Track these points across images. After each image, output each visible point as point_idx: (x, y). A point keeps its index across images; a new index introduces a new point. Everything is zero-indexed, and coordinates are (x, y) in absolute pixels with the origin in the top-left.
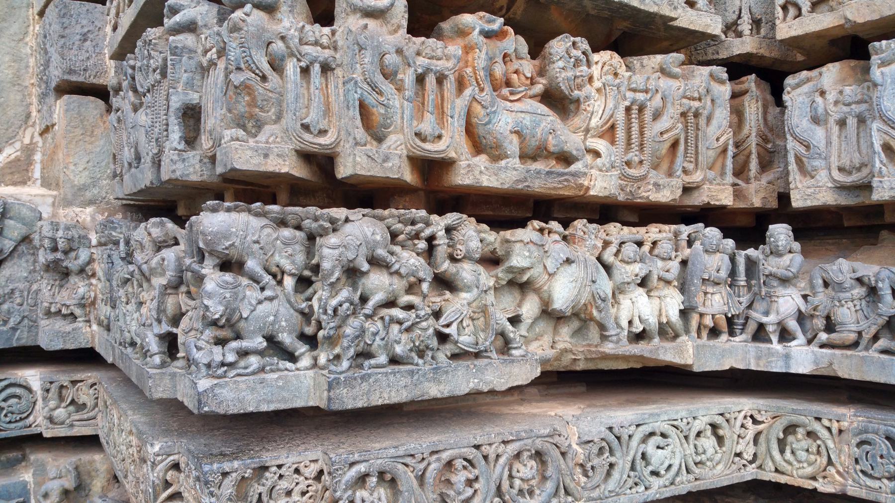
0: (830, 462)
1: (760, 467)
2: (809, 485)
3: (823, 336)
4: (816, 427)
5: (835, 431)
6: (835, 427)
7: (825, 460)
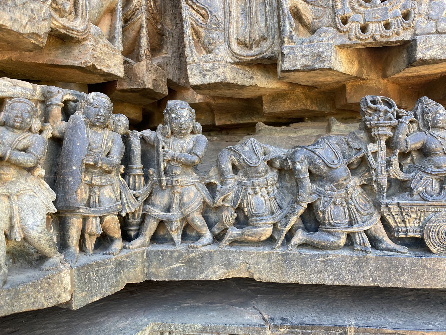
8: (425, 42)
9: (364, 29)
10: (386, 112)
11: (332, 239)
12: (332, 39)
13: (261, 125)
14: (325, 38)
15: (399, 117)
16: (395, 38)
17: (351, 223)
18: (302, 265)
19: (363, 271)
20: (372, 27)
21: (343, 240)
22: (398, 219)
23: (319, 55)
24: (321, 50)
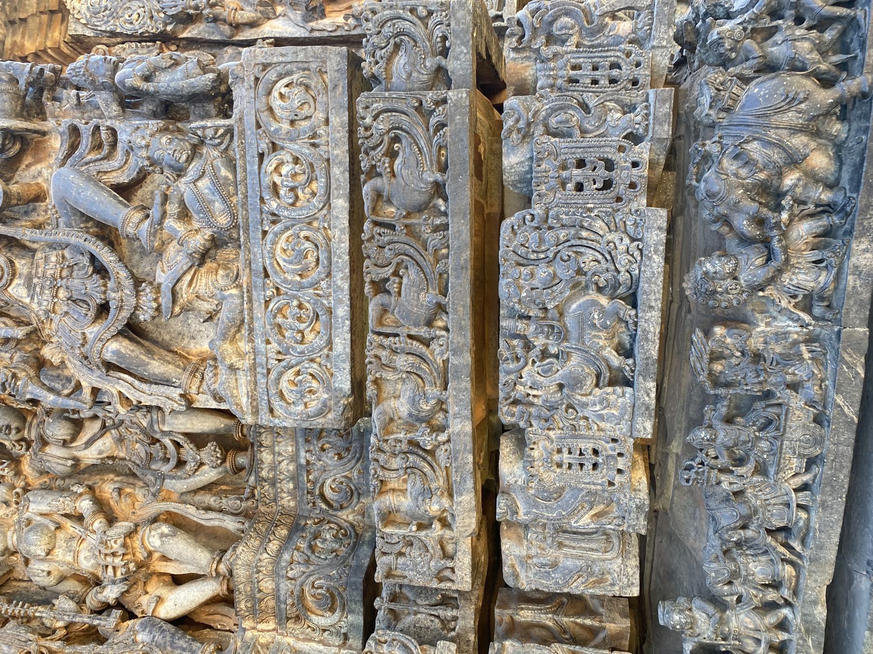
3: (786, 593)
8: (639, 432)
9: (620, 471)
10: (697, 473)
11: (801, 523)
12: (625, 496)
17: (788, 505)
18: (821, 548)
19: (832, 505)
20: (620, 467)
21: (803, 515)
23: (638, 507)
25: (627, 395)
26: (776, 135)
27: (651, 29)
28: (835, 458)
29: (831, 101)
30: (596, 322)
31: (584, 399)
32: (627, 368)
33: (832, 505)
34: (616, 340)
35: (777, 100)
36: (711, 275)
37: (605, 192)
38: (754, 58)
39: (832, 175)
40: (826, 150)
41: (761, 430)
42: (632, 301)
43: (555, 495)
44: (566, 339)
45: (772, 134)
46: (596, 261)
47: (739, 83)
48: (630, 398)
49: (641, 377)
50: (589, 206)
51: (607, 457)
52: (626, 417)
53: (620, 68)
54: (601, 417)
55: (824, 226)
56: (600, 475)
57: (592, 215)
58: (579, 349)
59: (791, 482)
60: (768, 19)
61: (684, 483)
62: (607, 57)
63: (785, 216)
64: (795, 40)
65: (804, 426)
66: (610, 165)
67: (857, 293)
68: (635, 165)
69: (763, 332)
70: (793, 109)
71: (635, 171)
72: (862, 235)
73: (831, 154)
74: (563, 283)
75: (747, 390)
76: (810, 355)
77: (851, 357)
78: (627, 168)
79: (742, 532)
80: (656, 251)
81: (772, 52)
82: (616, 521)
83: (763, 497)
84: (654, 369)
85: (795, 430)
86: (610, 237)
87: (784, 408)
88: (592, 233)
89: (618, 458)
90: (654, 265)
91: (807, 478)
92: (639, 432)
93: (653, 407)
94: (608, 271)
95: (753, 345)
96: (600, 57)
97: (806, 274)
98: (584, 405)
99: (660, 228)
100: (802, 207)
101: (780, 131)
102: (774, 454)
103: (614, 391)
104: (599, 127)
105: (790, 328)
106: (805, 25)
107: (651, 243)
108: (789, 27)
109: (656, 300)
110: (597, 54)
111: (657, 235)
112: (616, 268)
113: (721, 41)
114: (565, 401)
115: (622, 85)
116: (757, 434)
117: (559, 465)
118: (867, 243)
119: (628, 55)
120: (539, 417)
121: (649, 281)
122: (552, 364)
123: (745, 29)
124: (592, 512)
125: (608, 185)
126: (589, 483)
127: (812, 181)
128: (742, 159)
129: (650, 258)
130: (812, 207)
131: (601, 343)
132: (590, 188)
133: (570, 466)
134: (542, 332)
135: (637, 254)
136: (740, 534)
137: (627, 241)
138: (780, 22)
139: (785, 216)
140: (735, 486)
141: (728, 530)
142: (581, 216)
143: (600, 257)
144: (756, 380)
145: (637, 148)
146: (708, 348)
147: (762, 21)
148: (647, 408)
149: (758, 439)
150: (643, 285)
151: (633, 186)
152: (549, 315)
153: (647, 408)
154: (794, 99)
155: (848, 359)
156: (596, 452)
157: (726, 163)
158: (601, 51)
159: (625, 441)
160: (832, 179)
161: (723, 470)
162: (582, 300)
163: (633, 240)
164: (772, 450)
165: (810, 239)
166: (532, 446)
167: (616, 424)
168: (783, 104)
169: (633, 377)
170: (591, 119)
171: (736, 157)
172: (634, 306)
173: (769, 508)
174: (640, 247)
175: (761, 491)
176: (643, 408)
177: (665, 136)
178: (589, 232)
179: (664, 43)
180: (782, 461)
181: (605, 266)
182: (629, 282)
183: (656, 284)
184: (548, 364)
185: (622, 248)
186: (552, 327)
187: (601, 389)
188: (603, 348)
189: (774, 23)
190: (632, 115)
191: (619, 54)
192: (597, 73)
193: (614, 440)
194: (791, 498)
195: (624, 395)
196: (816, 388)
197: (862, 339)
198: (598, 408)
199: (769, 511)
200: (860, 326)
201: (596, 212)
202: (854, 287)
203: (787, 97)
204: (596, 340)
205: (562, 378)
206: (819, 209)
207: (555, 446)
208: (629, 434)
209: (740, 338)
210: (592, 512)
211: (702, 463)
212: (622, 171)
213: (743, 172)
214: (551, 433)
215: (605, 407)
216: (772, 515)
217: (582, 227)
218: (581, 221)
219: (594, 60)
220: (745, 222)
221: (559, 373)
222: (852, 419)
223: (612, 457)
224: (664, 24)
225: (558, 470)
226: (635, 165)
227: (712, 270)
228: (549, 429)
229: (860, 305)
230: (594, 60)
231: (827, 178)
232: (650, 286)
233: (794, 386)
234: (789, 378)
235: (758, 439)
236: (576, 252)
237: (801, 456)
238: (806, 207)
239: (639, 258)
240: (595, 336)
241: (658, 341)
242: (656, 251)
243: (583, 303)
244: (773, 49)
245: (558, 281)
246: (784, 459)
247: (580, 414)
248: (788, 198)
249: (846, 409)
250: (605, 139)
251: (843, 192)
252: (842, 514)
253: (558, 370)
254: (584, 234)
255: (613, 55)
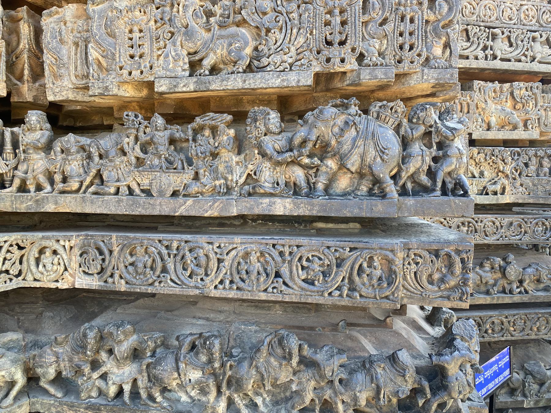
0: (66, 269)
1: (24, 279)
2: (53, 285)
3: (61, 186)
4: (56, 246)
5: (67, 247)
6: (67, 244)
7: (62, 268)
8: (159, 82)
9: (130, 73)
10: (133, 121)
11: (106, 189)
12: (114, 78)
13: (116, 126)
14: (111, 78)
15: (140, 124)
16: (145, 80)
17: (118, 180)
18: (92, 203)
19: (121, 206)
20: (133, 73)
21: (112, 190)
22: (140, 179)
23: (107, 87)
24: (107, 85)
25: (183, 73)
26: (361, 145)
27: (435, 68)
28: (151, 204)
29: (381, 176)
30: (233, 46)
31: (178, 43)
32: (202, 71)
33: (121, 206)
34: (222, 66)
35: (383, 143)
36: (268, 117)
37: (324, 41)
38: (412, 133)
39: (334, 191)
40: (350, 186)
41: (166, 159)
42: (249, 69)
43: (109, 30)
44: (221, 26)
45: (360, 142)
46: (276, 41)
47: (396, 123)
48: (182, 75)
49: (196, 79)
50: (314, 31)
51: (140, 63)
52: (168, 73)
53: (410, 50)
54: (167, 56)
55: (301, 185)
56: (126, 60)
57: (308, 35)
58: (213, 36)
59: (134, 182)
60: (437, 141)
61: (125, 113)
62: (418, 40)
63: (306, 161)
64: (422, 156)
65: (169, 185)
66: (342, 43)
67: (258, 205)
68: (343, 61)
69: (232, 160)
70: (377, 154)
71: (338, 60)
72: (295, 204)
73: (348, 190)
74: (260, 20)
75: (192, 147)
76: (217, 184)
77: (217, 207)
78: (340, 54)
79: (97, 154)
80: (283, 80)
81: (415, 145)
82: (95, 75)
83: (122, 167)
84: (203, 88)
85: (167, 179)
86: (293, 49)
87: (182, 171)
88: (295, 36)
89: (139, 71)
90: (274, 80)
91: (137, 191)
92: (159, 82)
93: (177, 90)
94: (269, 50)
95: (223, 155)
96: (418, 35)
97: (269, 175)
98: (174, 45)
99: (299, 81)
100: (313, 175)
101: (362, 147)
102: (151, 168)
103: (186, 63)
104: (369, 34)
105: (235, 175)
106: (432, 163)
107: (289, 77)
108: (431, 153)
109: (249, 84)
110: (420, 32)
111: (294, 80)
112: (271, 55)
113: (425, 109)
114: (176, 29)
115: (398, 52)
116: (163, 156)
117: (131, 31)
118: (290, 207)
119: (419, 55)
120: (163, 12)
121: (262, 78)
122: (202, 17)
123: (431, 126)
124: (100, 58)
125: (329, 43)
126: (120, 52)
127: (330, 177)
128: (344, 127)
129: (278, 77)
130: (314, 181)
131: (218, 51)
132: (327, 31)
133: (131, 39)
134: (224, 10)
135: (281, 68)
136: (95, 153)
137: (290, 61)
138: (435, 148)
139: (306, 161)
140: (127, 146)
141: (97, 145)
142: (307, 27)
143: (278, 44)
144: (199, 152)
145: (354, 60)
146: (219, 123)
147: (436, 137)
148: (175, 86)
149: (160, 157)
150: (259, 75)
151: (328, 60)
152: (237, 15)
153: (175, 86)
154: (383, 153)
155: (216, 205)
156: (141, 57)
157: (343, 118)
158: (422, 35)
159: (152, 75)
160: (331, 192)
161: (137, 139)
162: (249, 36)
163: (291, 65)
164: (153, 166)
165: (293, 179)
166: (142, 10)
167: (163, 67)
168: (381, 147)
169: (196, 76)
170: (375, 27)
171: (346, 123)
172: (244, 72)
173: (115, 170)
174: (286, 70)
175: (126, 166)
176: (175, 84)
177: (361, 78)
178: (296, 34)
179: (425, 77)
180: (146, 173)
181: (272, 47)
182: (262, 65)
183: (261, 83)
184: (202, 15)
185: (285, 58)
186: (228, 17)
187: (187, 55)
188: (215, 53)
189: (434, 144)
190: (377, 55)
191: (420, 47)
192: (407, 34)
193: (151, 68)
194: (123, 182)
195: (184, 70)
196: (196, 189)
197: (229, 212)
198: (173, 54)
199: (113, 170)
200: (237, 209)
201: (309, 36)
202: (262, 203)
203: (385, 149)
204: (220, 48)
205: (192, 27)
206: (312, 185)
207: (143, 27)
208: (157, 76)
209: (227, 144)
210: (100, 58)
211: (140, 124)
212: (339, 51)
213: (336, 130)
214: (152, 23)
215: (174, 58)
216: (110, 171)
217: (300, 29)
218: (303, 27)
219: (416, 31)
220: (303, 134)
221: (196, 25)
222: (178, 211)
223: (140, 66)
224: (438, 76)
225: (127, 31)
226: (343, 61)
227: (271, 117)
228: (156, 22)
229: (250, 208)
230: (416, 31)
231: (332, 189)
232: (259, 78)
233: (196, 177)
234: (201, 171)
235: (160, 157)
236: (281, 29)
237: (151, 184)
238: (313, 177)
239: (278, 70)
240: (223, 46)
241: (222, 88)
242: (283, 80)
243: (246, 36)
244: (417, 145)
245: (261, 16)
246: (148, 174)
247: (167, 42)
248: (319, 162)
249: (183, 207)
250: (361, 40)
251: (323, 194)
252: (115, 213)
253: (197, 24)
254: (295, 31)
255: (420, 46)
